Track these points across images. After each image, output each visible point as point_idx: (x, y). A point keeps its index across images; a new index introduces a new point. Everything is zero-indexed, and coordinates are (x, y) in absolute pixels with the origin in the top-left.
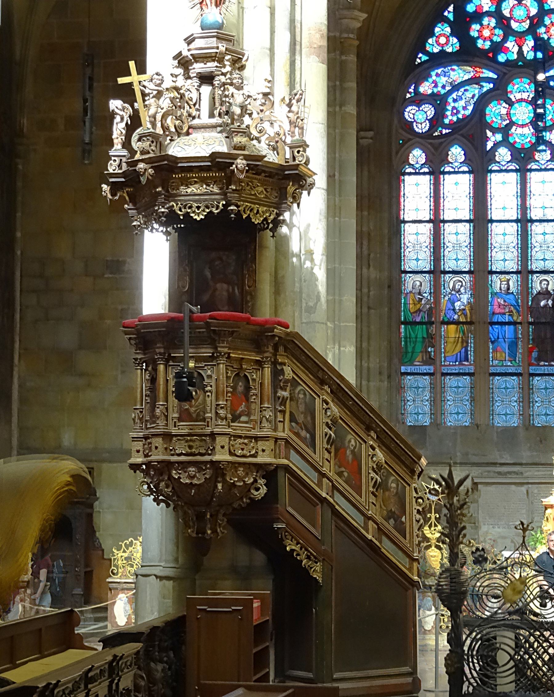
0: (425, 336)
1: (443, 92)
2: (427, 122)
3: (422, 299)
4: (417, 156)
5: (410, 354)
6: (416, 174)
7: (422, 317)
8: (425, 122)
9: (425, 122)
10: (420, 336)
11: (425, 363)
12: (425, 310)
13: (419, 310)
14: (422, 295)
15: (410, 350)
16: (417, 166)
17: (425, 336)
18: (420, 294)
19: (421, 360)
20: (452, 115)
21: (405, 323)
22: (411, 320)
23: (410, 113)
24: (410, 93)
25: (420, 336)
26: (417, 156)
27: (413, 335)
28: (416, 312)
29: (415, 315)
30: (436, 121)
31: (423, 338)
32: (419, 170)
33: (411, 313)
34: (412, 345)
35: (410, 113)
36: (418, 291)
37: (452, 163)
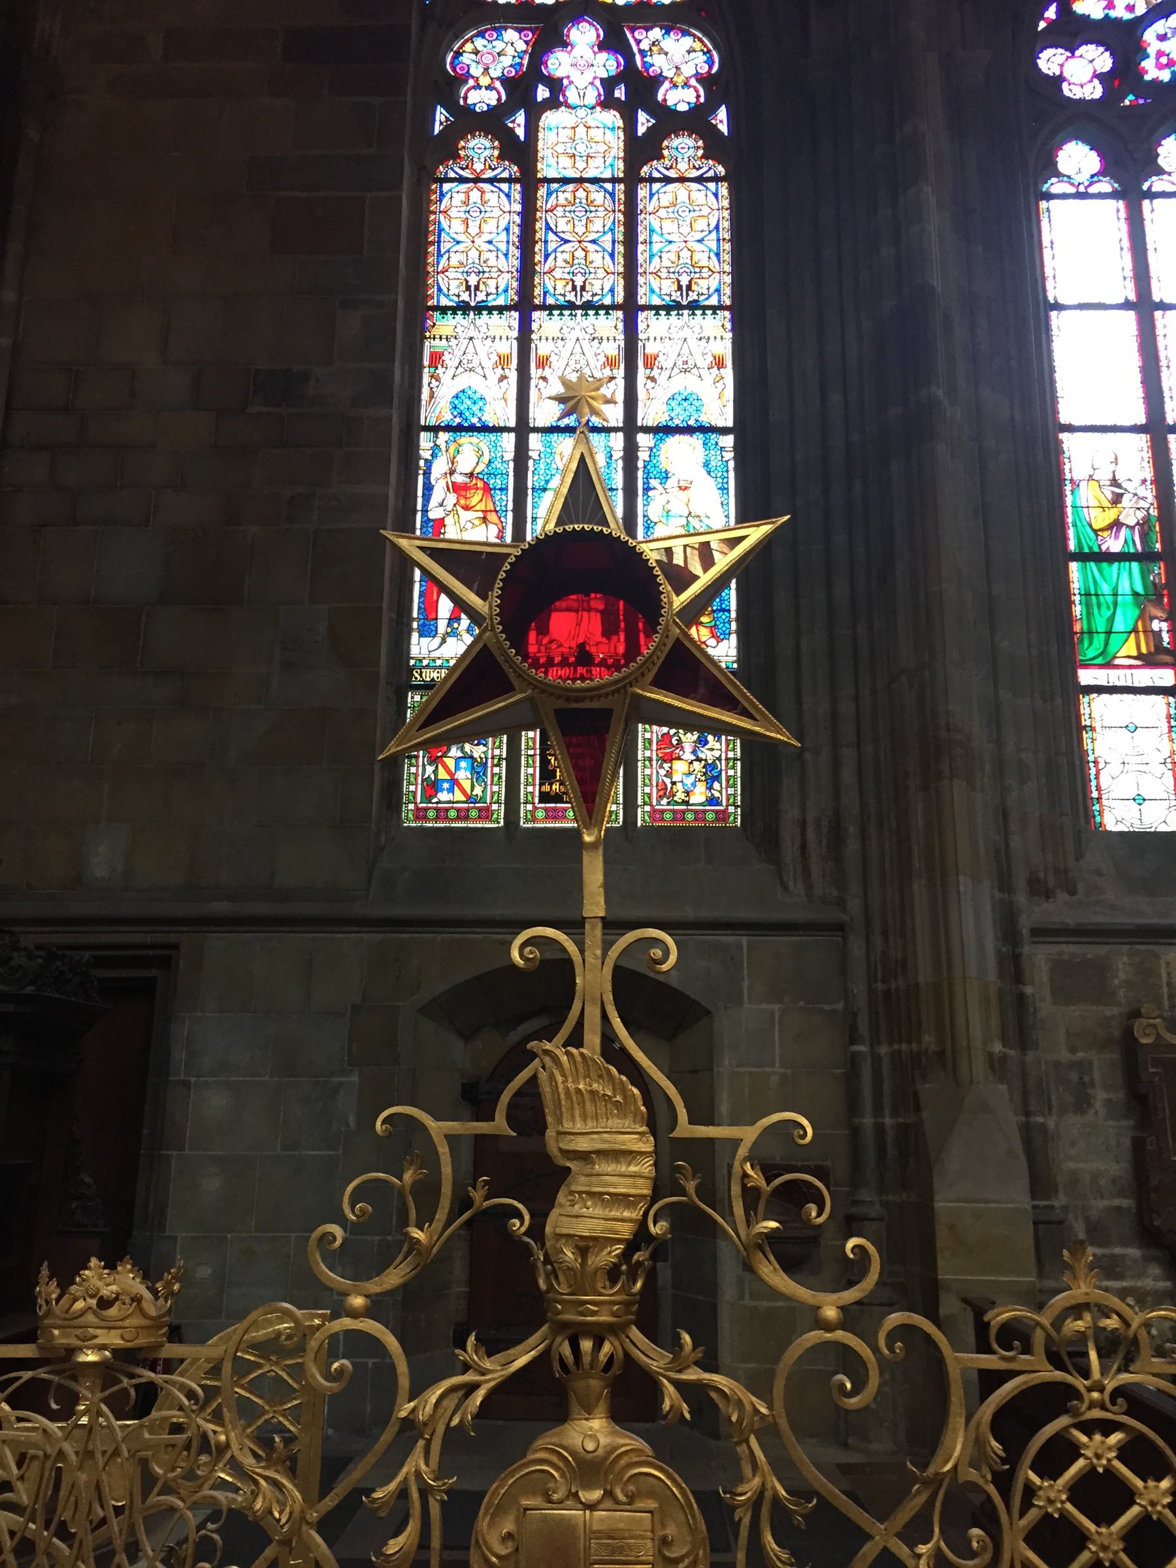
0: (1140, 589)
1: (1127, 16)
2: (1095, 80)
3: (1122, 495)
4: (1077, 159)
5: (1102, 636)
6: (1079, 196)
7: (1126, 541)
8: (1091, 81)
9: (1091, 81)
10: (1125, 587)
11: (1148, 661)
12: (1132, 523)
13: (1116, 525)
14: (1119, 486)
15: (1100, 625)
16: (1077, 179)
17: (1140, 589)
18: (1114, 482)
19: (1135, 653)
20: (1160, 67)
21: (1083, 557)
22: (1096, 549)
23: (1050, 61)
24: (1047, 20)
25: (1125, 587)
26: (1077, 159)
27: (1106, 588)
28: (1110, 527)
29: (1105, 534)
30: (1124, 73)
31: (1136, 594)
32: (1086, 188)
33: (1095, 531)
34: (1107, 614)
35: (1050, 61)
36: (1110, 476)
37: (1170, 174)
